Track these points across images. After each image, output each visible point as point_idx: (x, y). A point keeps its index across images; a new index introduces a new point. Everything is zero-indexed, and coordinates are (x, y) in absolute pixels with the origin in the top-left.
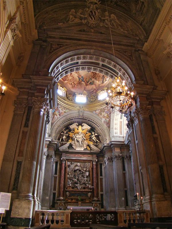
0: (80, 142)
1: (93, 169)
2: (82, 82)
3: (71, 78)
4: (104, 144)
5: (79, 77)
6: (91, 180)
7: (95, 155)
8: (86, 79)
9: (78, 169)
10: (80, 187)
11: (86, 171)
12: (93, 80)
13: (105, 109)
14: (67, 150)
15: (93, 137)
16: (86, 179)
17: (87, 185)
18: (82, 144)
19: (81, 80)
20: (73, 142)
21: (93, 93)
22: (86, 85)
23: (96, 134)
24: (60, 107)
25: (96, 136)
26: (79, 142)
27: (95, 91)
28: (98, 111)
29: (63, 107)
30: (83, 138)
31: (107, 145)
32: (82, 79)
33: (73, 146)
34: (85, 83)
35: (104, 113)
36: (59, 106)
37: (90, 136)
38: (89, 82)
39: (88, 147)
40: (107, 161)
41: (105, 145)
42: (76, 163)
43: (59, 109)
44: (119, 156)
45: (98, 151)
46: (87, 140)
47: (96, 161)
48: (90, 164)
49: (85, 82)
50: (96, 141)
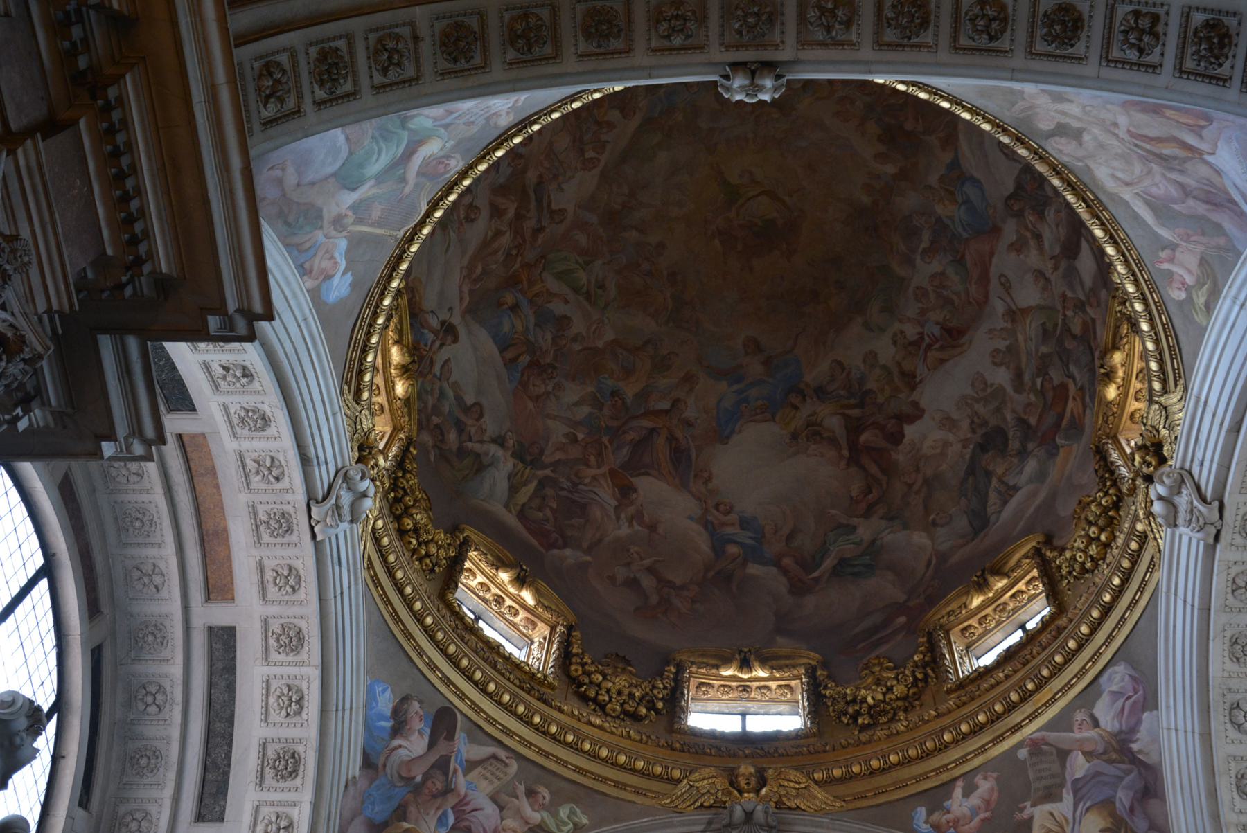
2: (754, 569)
3: (624, 531)
5: (706, 524)
8: (790, 537)
12: (864, 531)
13: (1063, 755)
19: (732, 549)
21: (879, 643)
22: (799, 589)
24: (470, 766)
27: (902, 619)
28: (975, 800)
29: (514, 766)
32: (745, 537)
34: (785, 571)
35: (1064, 806)
36: (464, 748)
38: (828, 563)
43: (461, 781)
49: (787, 561)
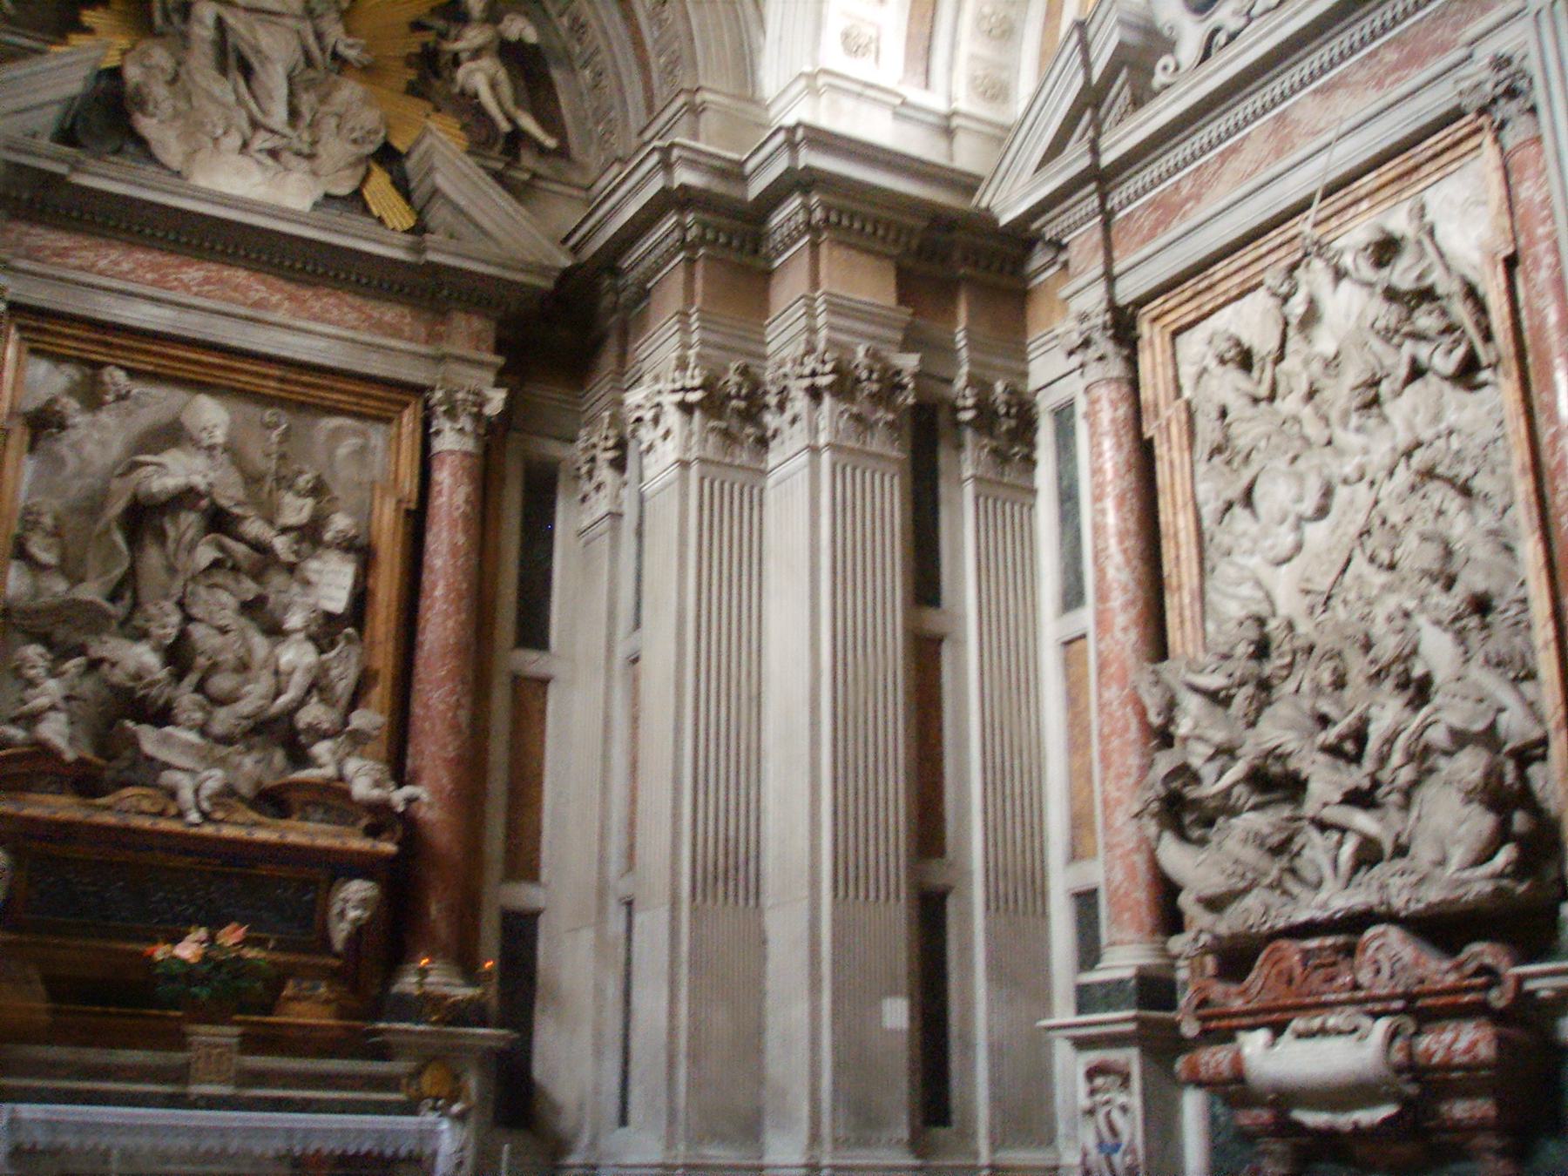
0: (275, 80)
1: (417, 521)
4: (666, 165)
6: (380, 693)
7: (477, 324)
9: (186, 498)
10: (214, 779)
11: (311, 534)
14: (52, 160)
15: (476, 54)
16: (297, 656)
17: (322, 749)
18: (294, 114)
20: (160, 56)
23: (519, 28)
25: (513, 54)
26: (247, 71)
30: (319, 36)
31: (719, 187)
33: (147, 126)
37: (418, 26)
39: (380, 191)
40: (672, 418)
41: (684, 176)
42: (159, 402)
44: (891, 384)
45: (543, 270)
46: (369, 72)
47: (478, 417)
48: (377, 436)
50: (511, 120)
